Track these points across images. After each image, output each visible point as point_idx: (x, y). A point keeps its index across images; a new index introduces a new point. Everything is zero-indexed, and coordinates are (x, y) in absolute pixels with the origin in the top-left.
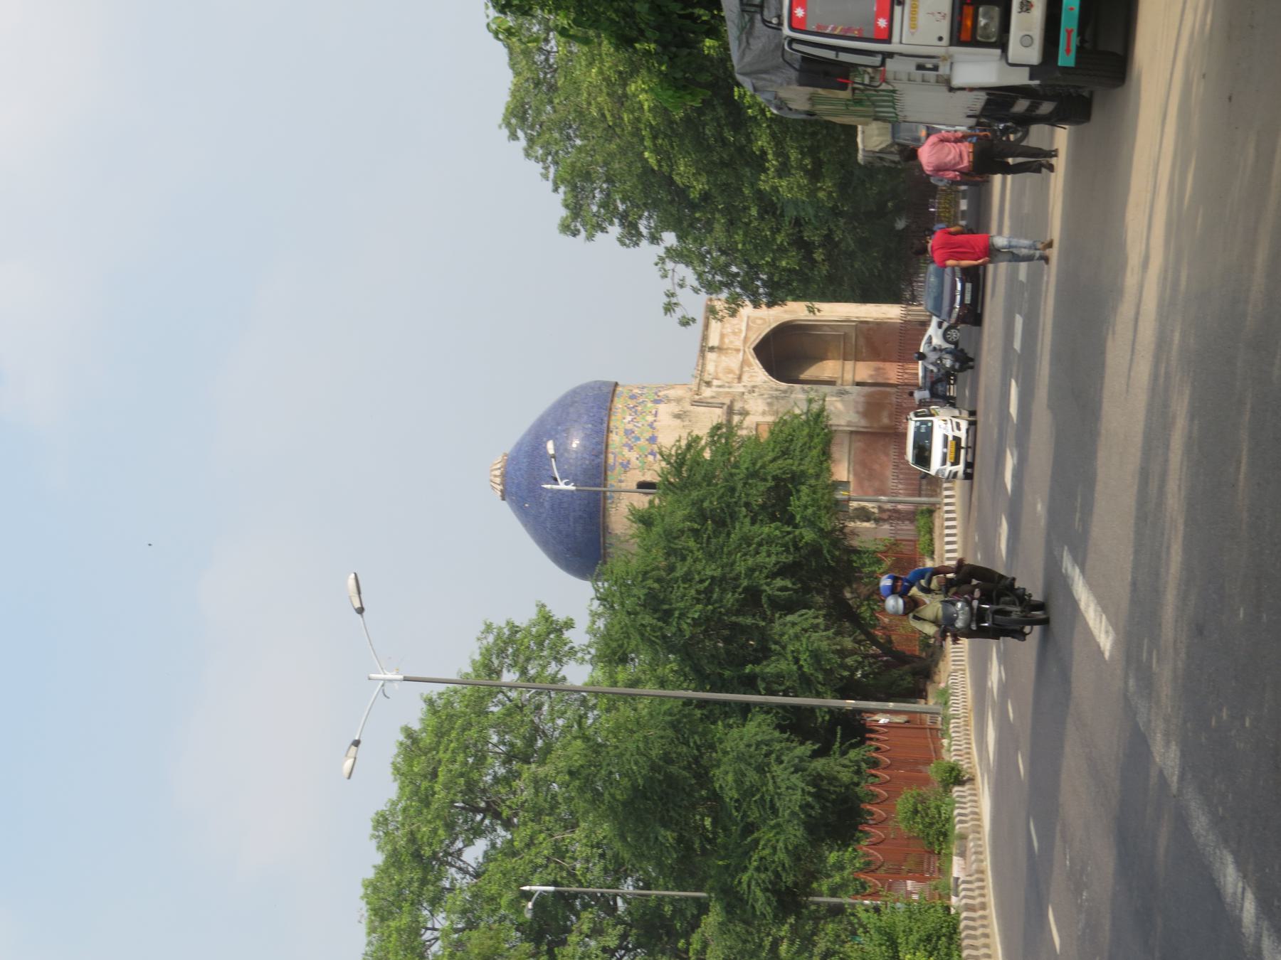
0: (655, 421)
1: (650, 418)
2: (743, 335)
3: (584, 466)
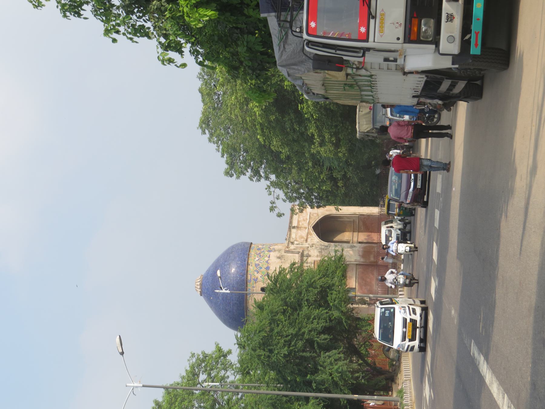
0: (269, 260)
1: (267, 259)
2: (308, 221)
3: (237, 280)
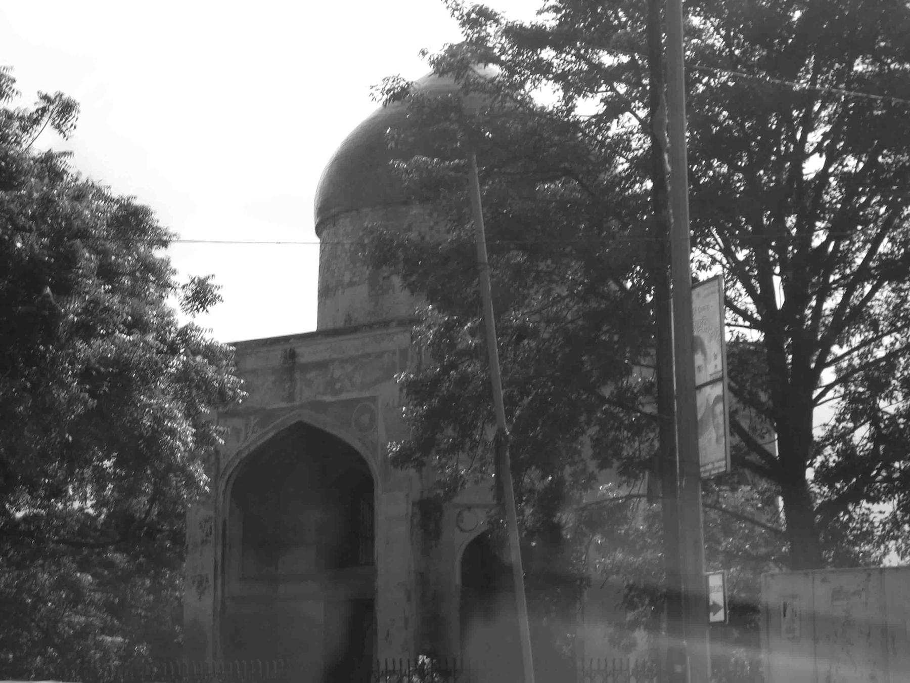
2: (329, 398)
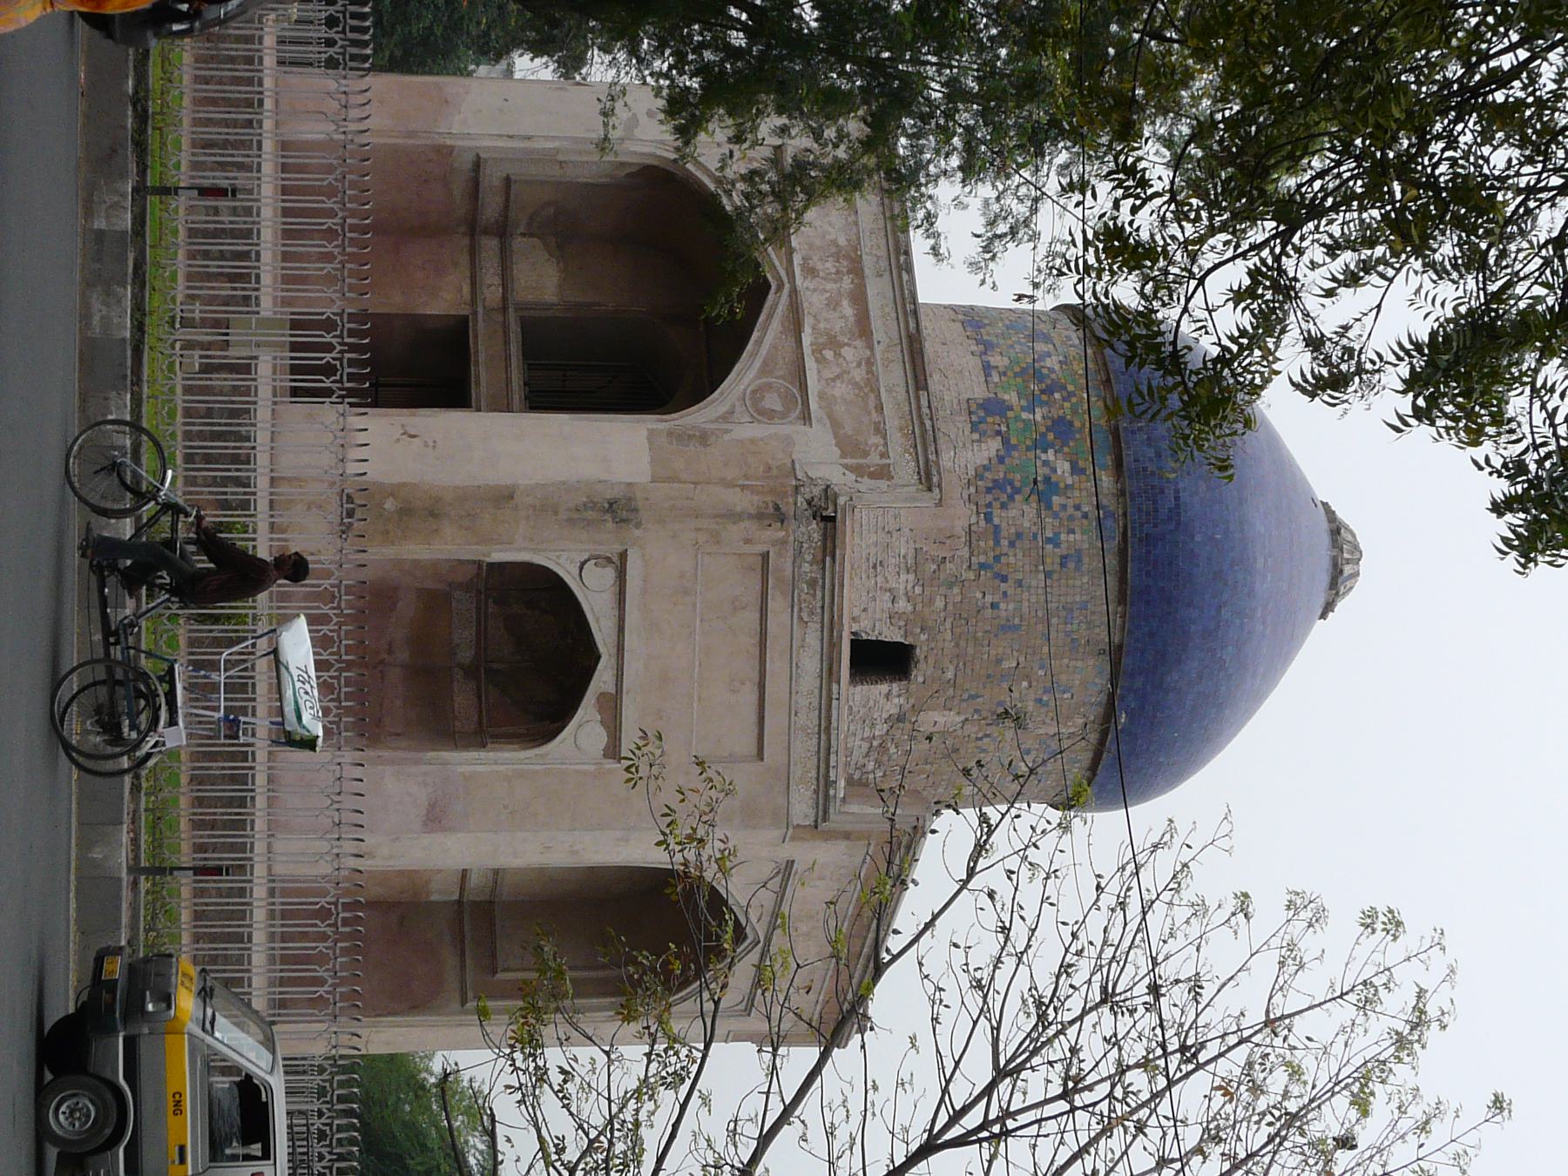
2: (807, 339)
